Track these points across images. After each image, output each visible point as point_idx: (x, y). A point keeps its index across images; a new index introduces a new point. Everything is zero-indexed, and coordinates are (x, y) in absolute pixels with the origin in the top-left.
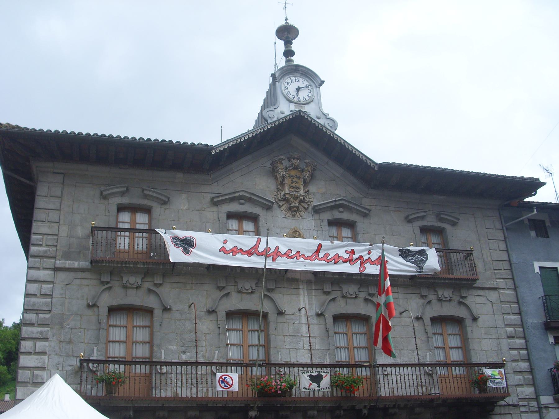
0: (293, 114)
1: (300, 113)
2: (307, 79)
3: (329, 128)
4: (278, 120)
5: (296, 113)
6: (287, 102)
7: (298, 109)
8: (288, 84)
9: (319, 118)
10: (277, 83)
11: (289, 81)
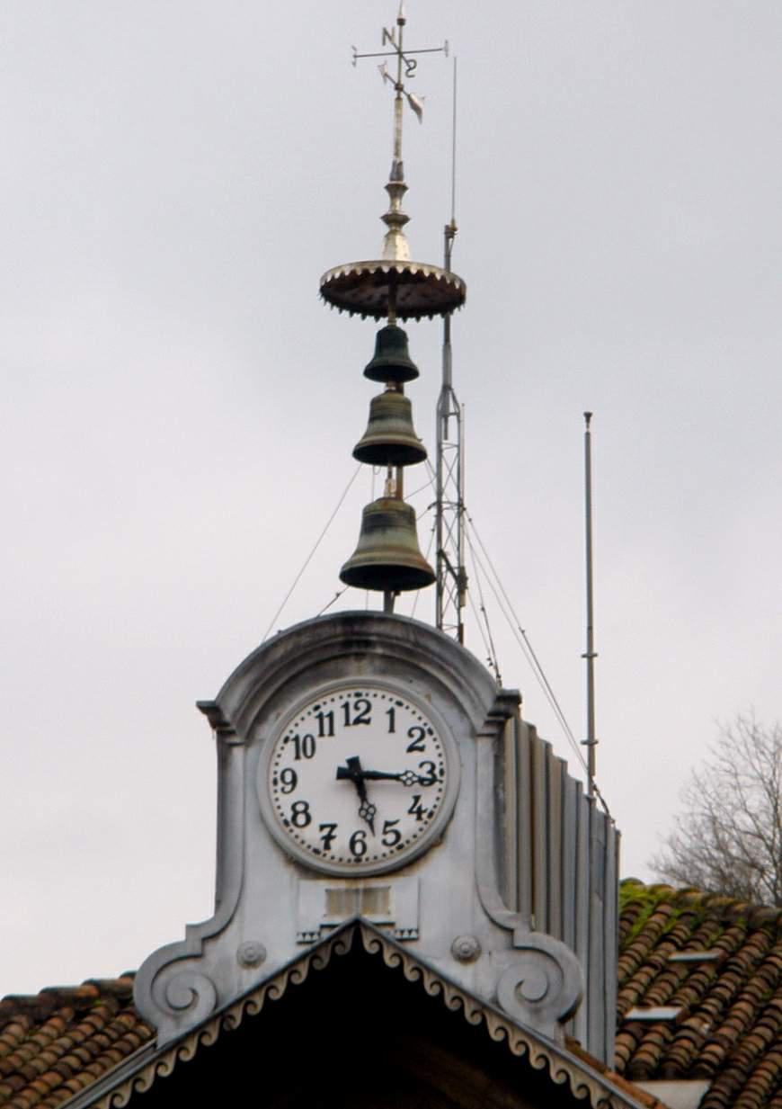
0: (311, 956)
1: (358, 940)
2: (417, 689)
3: (522, 1016)
4: (220, 1016)
5: (335, 940)
6: (286, 874)
7: (340, 920)
8: (304, 748)
9: (466, 958)
10: (238, 753)
11: (308, 726)
